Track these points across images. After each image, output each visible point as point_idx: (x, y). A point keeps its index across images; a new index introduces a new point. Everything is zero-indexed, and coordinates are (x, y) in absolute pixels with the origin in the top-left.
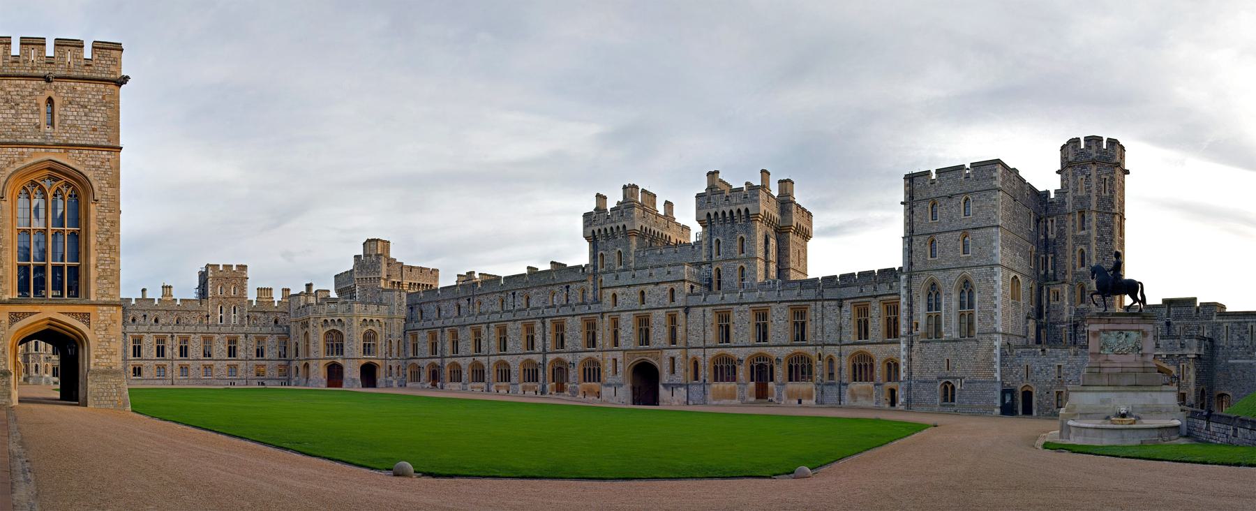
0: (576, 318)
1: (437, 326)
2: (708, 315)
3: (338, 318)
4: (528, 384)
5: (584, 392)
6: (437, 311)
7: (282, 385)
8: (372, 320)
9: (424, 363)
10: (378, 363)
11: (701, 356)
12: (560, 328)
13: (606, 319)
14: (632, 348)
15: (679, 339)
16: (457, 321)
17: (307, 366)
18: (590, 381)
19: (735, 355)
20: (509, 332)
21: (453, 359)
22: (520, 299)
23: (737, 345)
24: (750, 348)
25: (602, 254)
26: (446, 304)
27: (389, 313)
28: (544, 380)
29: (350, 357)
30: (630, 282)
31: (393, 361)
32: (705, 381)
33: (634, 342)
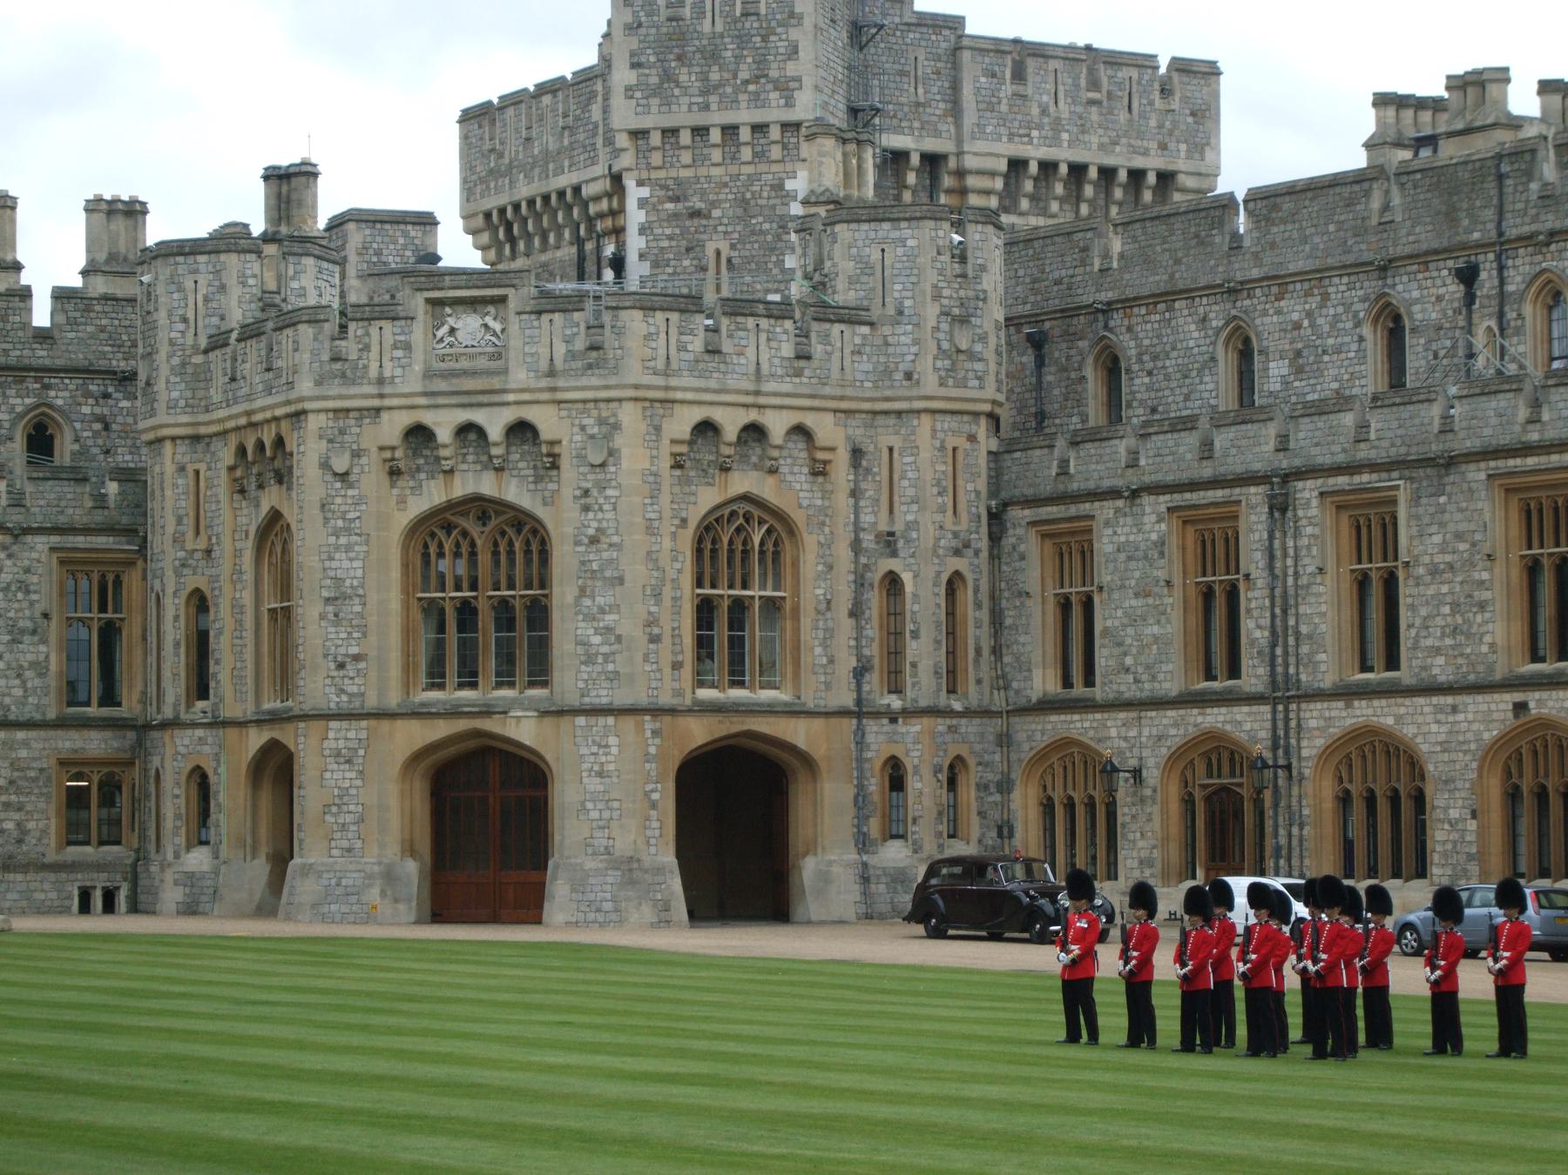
1: (1236, 464)
3: (508, 416)
6: (1226, 364)
8: (755, 432)
10: (801, 743)
21: (1364, 712)
26: (1294, 308)
29: (602, 696)
31: (916, 727)
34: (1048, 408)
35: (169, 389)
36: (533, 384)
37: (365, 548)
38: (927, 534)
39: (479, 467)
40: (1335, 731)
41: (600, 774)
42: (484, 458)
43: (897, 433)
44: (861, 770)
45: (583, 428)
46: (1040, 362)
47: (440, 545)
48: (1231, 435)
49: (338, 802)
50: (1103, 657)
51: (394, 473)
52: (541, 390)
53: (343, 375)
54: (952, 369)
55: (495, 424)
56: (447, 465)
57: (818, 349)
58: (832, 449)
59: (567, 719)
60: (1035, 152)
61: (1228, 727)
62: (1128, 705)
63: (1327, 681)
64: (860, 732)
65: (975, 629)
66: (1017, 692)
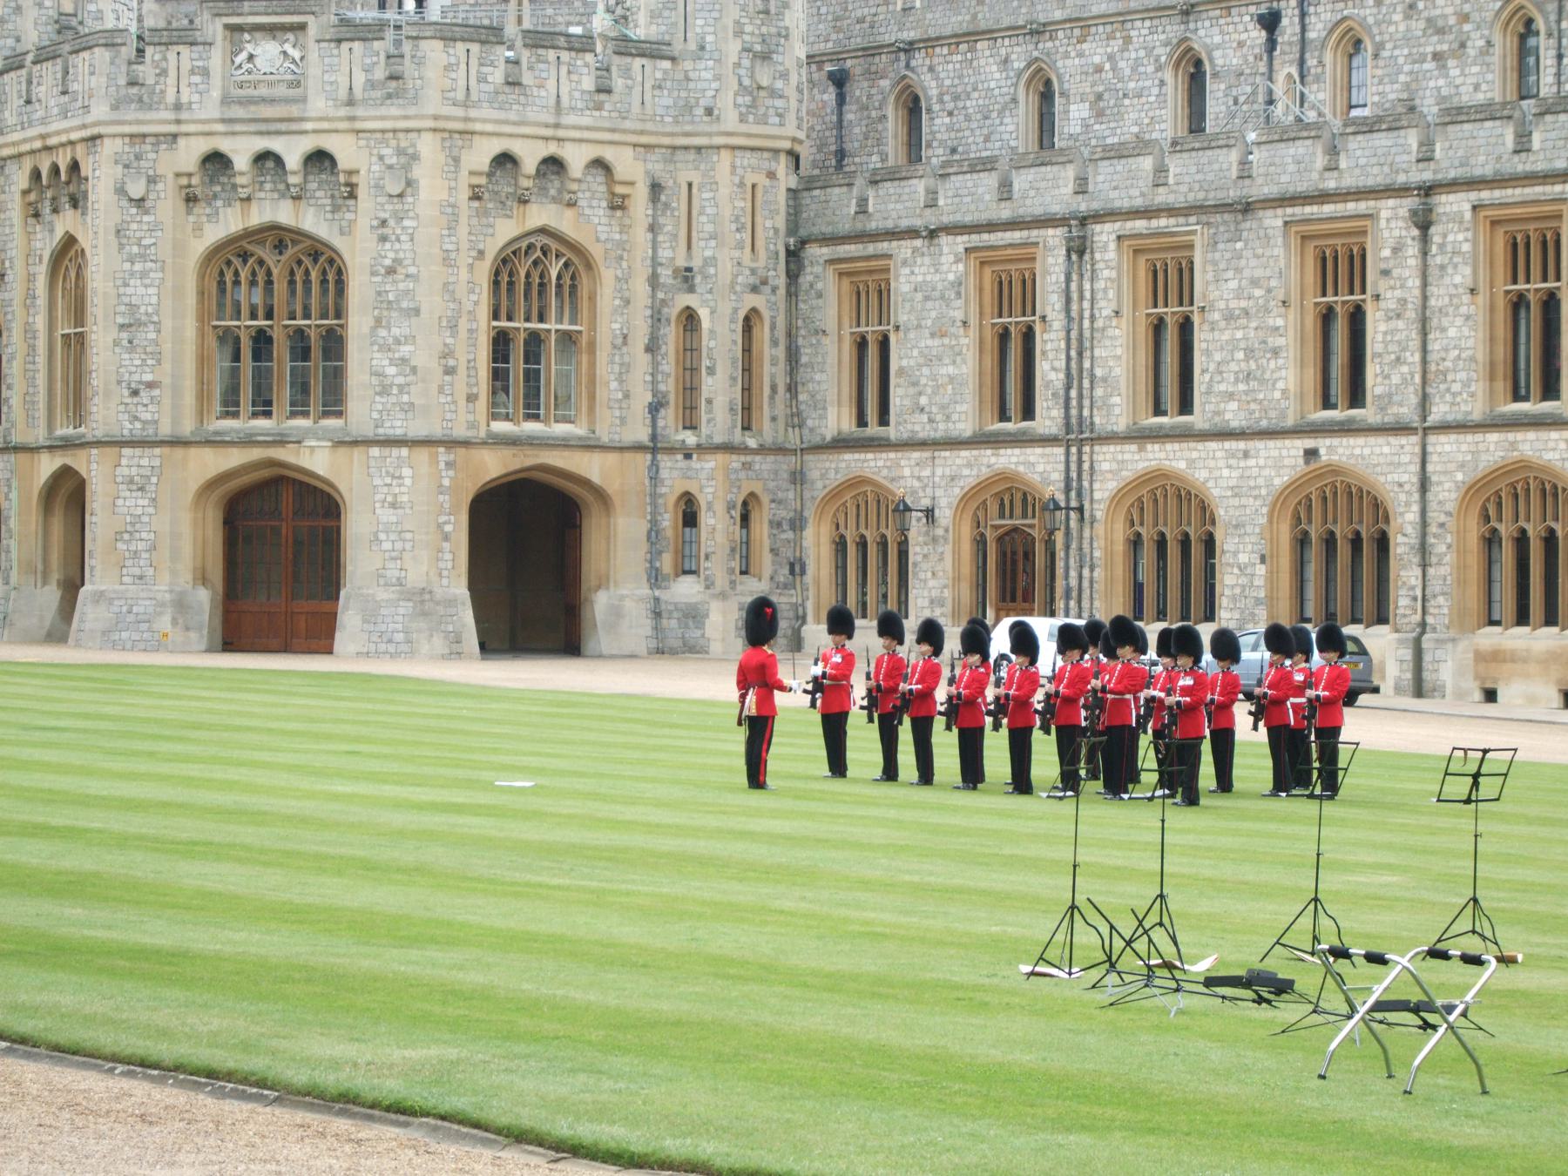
1: (1034, 206)
3: (307, 144)
6: (1027, 107)
8: (553, 165)
10: (596, 479)
29: (397, 426)
31: (710, 463)
34: (848, 146)
36: (332, 113)
37: (160, 275)
38: (725, 270)
39: (276, 196)
40: (1128, 475)
41: (393, 505)
42: (282, 187)
43: (697, 169)
44: (654, 504)
45: (381, 158)
46: (841, 100)
47: (236, 273)
48: (1030, 178)
49: (128, 531)
51: (191, 199)
52: (341, 119)
53: (140, 100)
54: (753, 105)
55: (293, 153)
56: (243, 193)
58: (632, 184)
59: (357, 452)
61: (1021, 469)
62: (923, 444)
63: (1121, 424)
64: (655, 467)
66: (811, 430)
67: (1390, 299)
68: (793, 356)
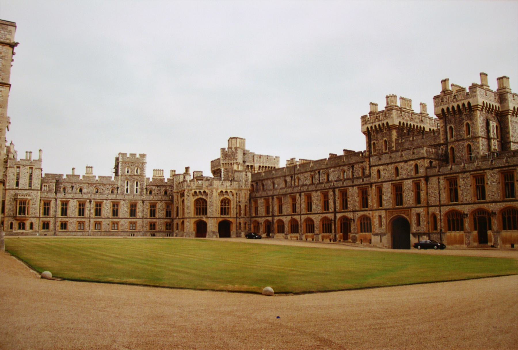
0: (355, 188)
2: (442, 182)
4: (325, 234)
5: (361, 240)
7: (167, 236)
8: (226, 192)
9: (262, 220)
11: (437, 212)
12: (344, 195)
13: (374, 188)
14: (391, 208)
15: (422, 200)
16: (282, 192)
17: (183, 223)
18: (365, 232)
19: (462, 210)
20: (313, 198)
22: (323, 175)
23: (463, 203)
24: (472, 205)
25: (374, 143)
26: (278, 180)
27: (239, 186)
28: (335, 232)
29: (211, 216)
30: (388, 161)
31: (241, 219)
32: (441, 230)
33: (392, 203)
35: (175, 187)
49: (187, 226)
50: (259, 213)
55: (202, 191)
57: (232, 184)
60: (261, 165)
65: (248, 209)
67: (298, 203)
68: (250, 209)
